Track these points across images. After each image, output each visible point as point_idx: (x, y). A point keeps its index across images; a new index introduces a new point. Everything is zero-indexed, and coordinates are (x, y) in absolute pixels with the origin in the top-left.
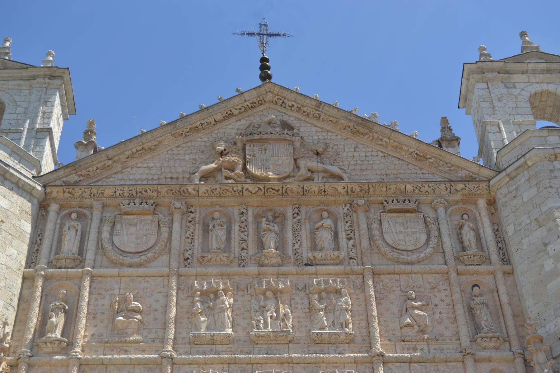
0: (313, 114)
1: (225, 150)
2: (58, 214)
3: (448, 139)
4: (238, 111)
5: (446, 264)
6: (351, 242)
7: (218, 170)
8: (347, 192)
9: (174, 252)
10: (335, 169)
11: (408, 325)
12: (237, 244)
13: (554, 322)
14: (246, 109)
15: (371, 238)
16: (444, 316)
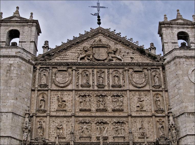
0: (113, 38)
1: (87, 50)
2: (39, 70)
3: (153, 47)
4: (91, 36)
5: (150, 88)
6: (124, 81)
7: (85, 56)
8: (123, 65)
9: (74, 83)
10: (119, 57)
11: (138, 107)
12: (91, 81)
13: (176, 107)
14: (93, 35)
15: (129, 80)
16: (148, 104)
